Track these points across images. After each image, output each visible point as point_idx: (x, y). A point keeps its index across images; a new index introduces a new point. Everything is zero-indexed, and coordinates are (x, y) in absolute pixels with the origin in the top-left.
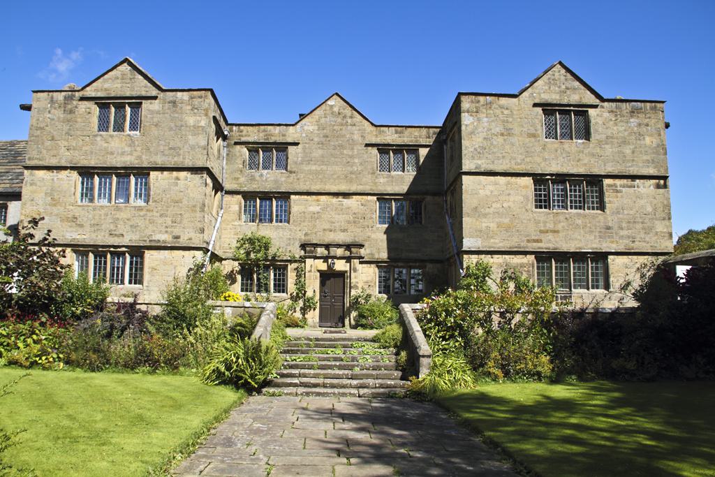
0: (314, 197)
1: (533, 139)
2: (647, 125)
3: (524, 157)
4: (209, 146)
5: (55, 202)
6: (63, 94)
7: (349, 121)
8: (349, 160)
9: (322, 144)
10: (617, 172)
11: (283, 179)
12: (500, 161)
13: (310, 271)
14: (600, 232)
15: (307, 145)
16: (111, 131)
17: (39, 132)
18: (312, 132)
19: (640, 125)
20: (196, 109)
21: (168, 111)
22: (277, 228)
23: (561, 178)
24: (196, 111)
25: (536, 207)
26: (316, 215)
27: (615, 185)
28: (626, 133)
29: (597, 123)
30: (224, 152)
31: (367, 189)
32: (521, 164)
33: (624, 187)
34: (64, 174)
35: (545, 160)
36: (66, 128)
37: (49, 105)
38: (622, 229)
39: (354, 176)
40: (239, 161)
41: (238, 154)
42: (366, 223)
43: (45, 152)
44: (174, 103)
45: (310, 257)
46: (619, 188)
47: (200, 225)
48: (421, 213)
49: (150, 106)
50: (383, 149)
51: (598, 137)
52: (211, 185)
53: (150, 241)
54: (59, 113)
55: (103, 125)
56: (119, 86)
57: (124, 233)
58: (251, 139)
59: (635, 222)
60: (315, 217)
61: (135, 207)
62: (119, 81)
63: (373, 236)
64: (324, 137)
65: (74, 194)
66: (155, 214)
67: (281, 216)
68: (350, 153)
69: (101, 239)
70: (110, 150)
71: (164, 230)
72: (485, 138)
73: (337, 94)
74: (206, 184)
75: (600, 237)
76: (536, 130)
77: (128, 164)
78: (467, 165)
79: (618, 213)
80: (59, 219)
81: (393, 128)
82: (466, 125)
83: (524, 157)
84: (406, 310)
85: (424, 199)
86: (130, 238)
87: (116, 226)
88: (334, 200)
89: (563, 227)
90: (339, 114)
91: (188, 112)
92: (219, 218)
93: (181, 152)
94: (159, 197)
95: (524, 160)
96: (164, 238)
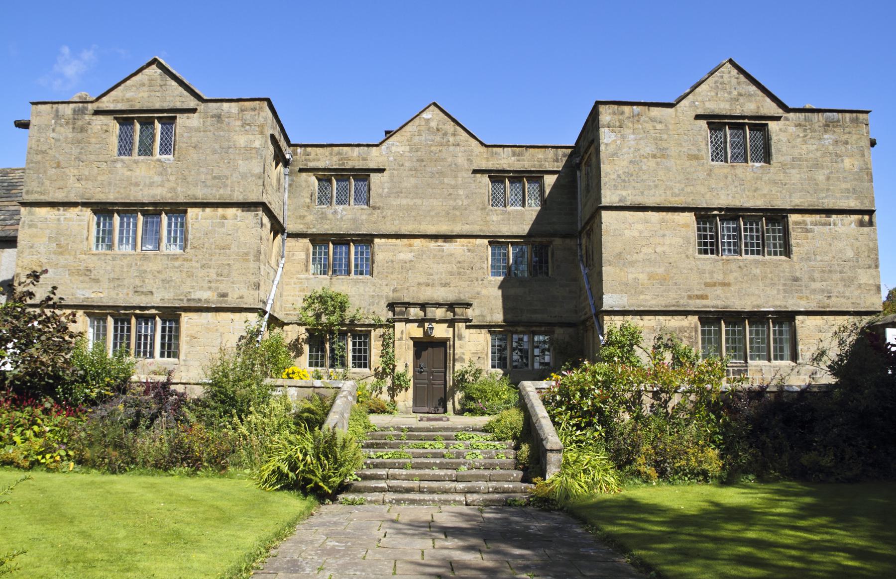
0: (405, 241)
1: (695, 163)
2: (847, 143)
3: (683, 186)
4: (266, 174)
5: (61, 250)
6: (72, 106)
7: (451, 139)
8: (451, 191)
9: (415, 170)
10: (806, 204)
11: (364, 217)
12: (652, 192)
13: (401, 339)
14: (785, 285)
15: (395, 172)
16: (135, 156)
17: (39, 157)
18: (402, 155)
19: (836, 142)
20: (249, 124)
21: (211, 128)
22: (356, 282)
23: (732, 214)
24: (248, 127)
25: (700, 252)
26: (408, 265)
28: (819, 154)
29: (779, 140)
30: (286, 182)
31: (475, 229)
32: (679, 195)
33: (816, 225)
34: (73, 212)
35: (711, 190)
36: (75, 151)
37: (53, 121)
38: (814, 280)
39: (458, 213)
40: (306, 194)
41: (304, 184)
42: (475, 275)
43: (47, 183)
44: (219, 117)
45: (400, 320)
46: (809, 227)
47: (253, 279)
48: (547, 262)
49: (189, 121)
50: (497, 176)
51: (781, 159)
52: (269, 225)
53: (189, 300)
54: (66, 132)
55: (125, 147)
56: (146, 95)
57: (154, 290)
58: (321, 165)
59: (830, 271)
60: (406, 267)
61: (168, 255)
62: (146, 88)
63: (484, 292)
64: (418, 161)
65: (87, 239)
66: (195, 264)
67: (362, 265)
68: (453, 182)
69: (123, 297)
70: (134, 180)
71: (206, 285)
72: (631, 162)
73: (435, 104)
74: (262, 225)
75: (785, 291)
76: (698, 150)
77: (158, 199)
78: (608, 197)
79: (809, 259)
80: (67, 273)
81: (510, 149)
82: (607, 144)
83: (683, 186)
84: (528, 389)
85: (551, 242)
86: (161, 297)
87: (143, 281)
88: (432, 244)
89: (736, 278)
90: (438, 130)
91: (237, 129)
92: (280, 270)
93: (229, 182)
94: (200, 242)
95: (683, 190)
96: (206, 296)
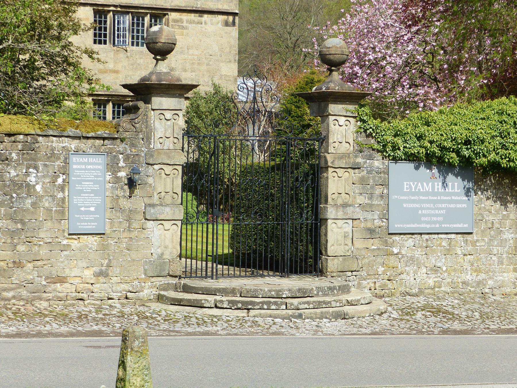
10: (183, 5)
27: (181, 21)
46: (185, 24)
